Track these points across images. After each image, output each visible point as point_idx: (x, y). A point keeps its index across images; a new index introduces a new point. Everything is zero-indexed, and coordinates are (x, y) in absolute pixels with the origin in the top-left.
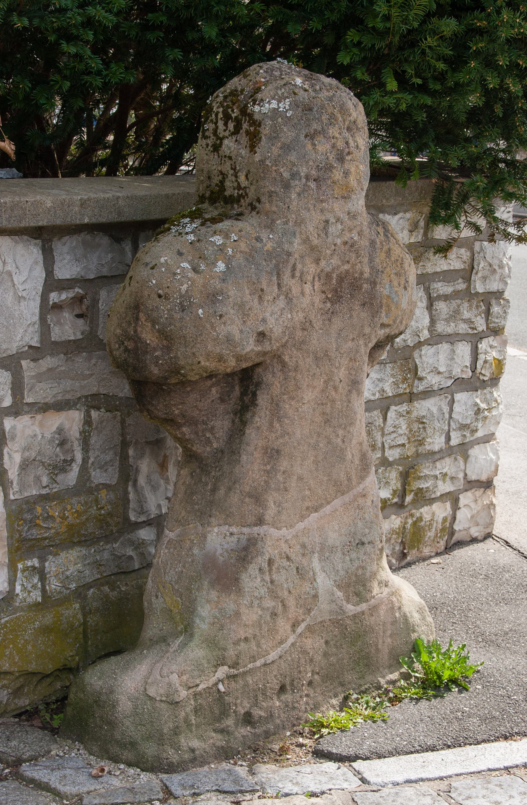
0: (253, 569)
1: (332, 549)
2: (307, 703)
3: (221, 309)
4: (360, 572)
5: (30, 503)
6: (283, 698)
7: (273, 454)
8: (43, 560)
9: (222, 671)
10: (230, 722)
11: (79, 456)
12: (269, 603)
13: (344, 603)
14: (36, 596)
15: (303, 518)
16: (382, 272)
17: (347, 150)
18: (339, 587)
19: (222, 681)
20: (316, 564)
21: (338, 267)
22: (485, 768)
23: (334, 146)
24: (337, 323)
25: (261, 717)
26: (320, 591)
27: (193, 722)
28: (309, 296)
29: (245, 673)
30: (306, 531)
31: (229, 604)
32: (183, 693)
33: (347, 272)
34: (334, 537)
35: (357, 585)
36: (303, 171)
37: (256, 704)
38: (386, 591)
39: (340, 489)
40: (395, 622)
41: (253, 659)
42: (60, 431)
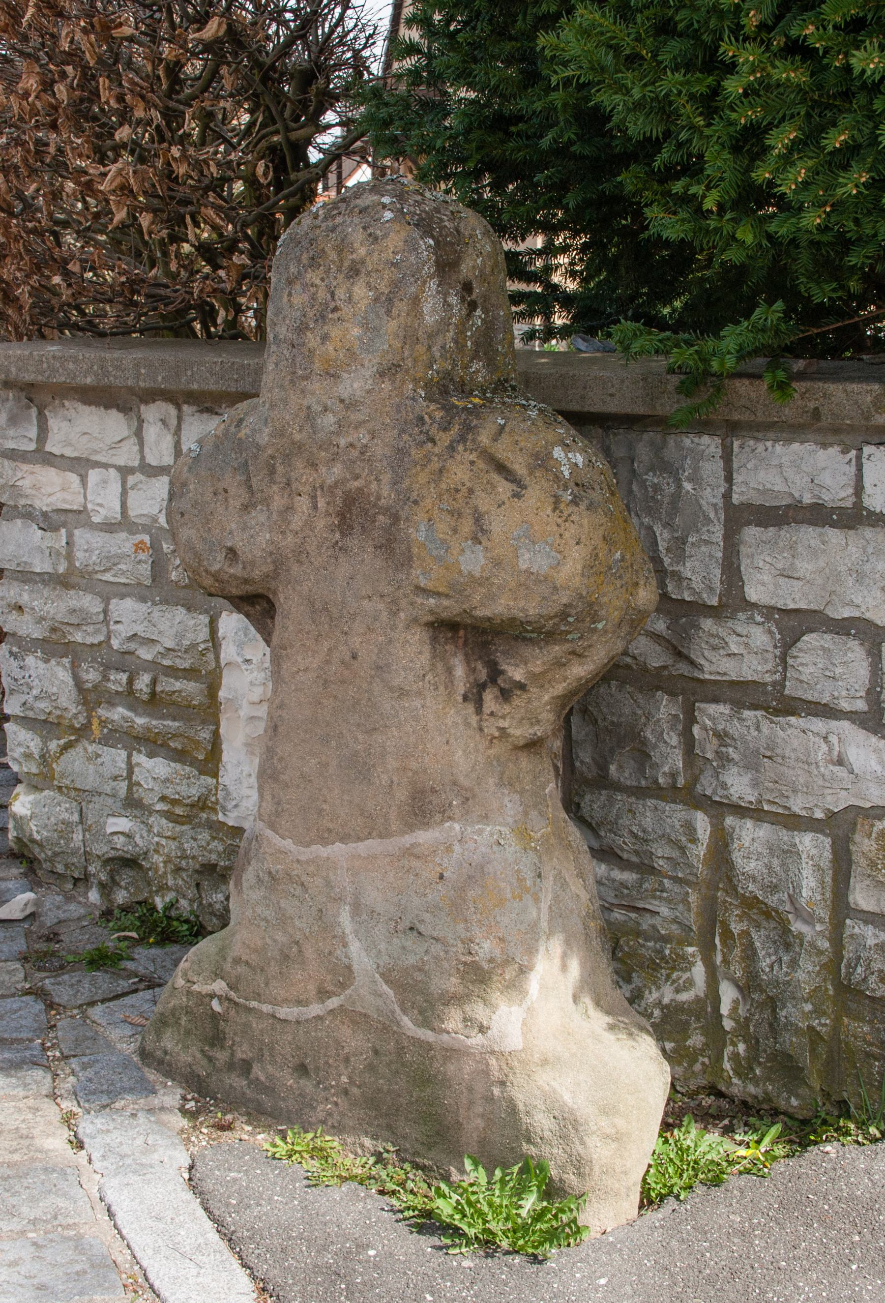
2: (330, 1114)
4: (419, 976)
6: (302, 1082)
9: (219, 986)
10: (222, 1056)
13: (398, 1009)
15: (325, 842)
16: (416, 502)
17: (332, 305)
18: (386, 977)
19: (220, 998)
20: (345, 919)
21: (344, 481)
22: (145, 1264)
23: (313, 298)
25: (257, 1079)
26: (355, 967)
27: (183, 1023)
28: (310, 516)
29: (249, 1010)
33: (360, 490)
34: (373, 897)
37: (260, 1058)
38: (476, 1040)
40: (490, 1099)
41: (258, 997)
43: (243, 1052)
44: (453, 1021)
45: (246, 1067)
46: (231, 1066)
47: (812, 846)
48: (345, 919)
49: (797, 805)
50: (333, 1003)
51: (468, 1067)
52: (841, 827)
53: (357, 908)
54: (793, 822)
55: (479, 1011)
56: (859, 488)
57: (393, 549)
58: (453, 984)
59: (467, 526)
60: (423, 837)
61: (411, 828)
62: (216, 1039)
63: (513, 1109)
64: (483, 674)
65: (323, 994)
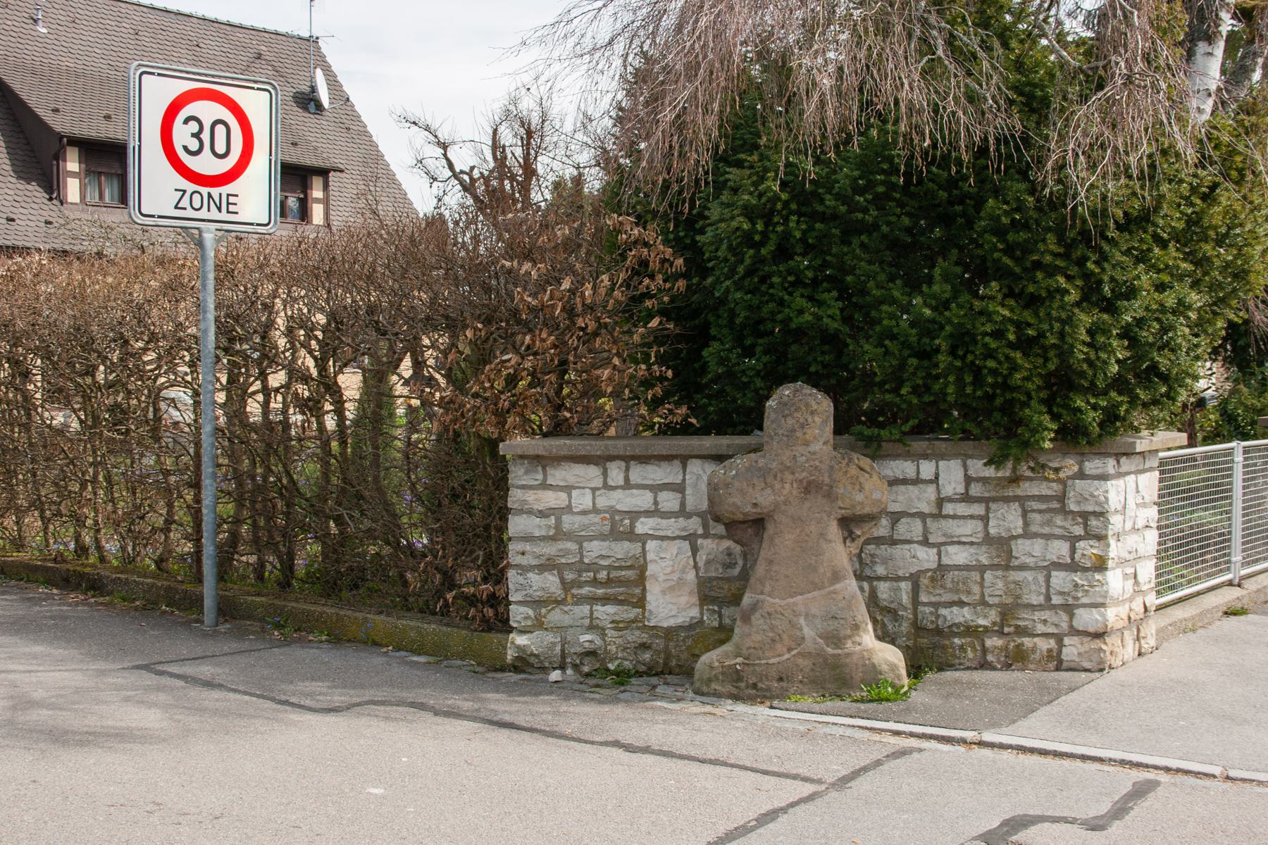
0: (757, 615)
1: (814, 616)
3: (730, 491)
5: (711, 579)
7: (771, 562)
8: (720, 608)
9: (739, 660)
10: (743, 685)
11: (740, 563)
12: (771, 634)
14: (716, 624)
15: (792, 597)
20: (802, 621)
24: (807, 504)
28: (789, 489)
30: (795, 604)
31: (746, 629)
32: (717, 664)
34: (814, 610)
35: (835, 639)
36: (781, 432)
37: (761, 681)
38: (858, 648)
39: (817, 587)
41: (760, 659)
42: (728, 548)
43: (752, 680)
44: (849, 644)
45: (755, 686)
46: (747, 687)
47: (905, 586)
48: (802, 621)
49: (900, 573)
50: (794, 652)
51: (855, 658)
52: (915, 579)
53: (807, 616)
54: (899, 579)
55: (857, 639)
56: (918, 473)
57: (830, 496)
58: (849, 632)
59: (857, 487)
60: (838, 586)
61: (833, 584)
62: (740, 679)
63: (874, 665)
64: (846, 534)
65: (790, 650)
